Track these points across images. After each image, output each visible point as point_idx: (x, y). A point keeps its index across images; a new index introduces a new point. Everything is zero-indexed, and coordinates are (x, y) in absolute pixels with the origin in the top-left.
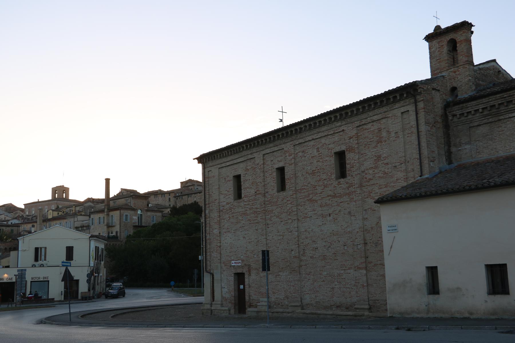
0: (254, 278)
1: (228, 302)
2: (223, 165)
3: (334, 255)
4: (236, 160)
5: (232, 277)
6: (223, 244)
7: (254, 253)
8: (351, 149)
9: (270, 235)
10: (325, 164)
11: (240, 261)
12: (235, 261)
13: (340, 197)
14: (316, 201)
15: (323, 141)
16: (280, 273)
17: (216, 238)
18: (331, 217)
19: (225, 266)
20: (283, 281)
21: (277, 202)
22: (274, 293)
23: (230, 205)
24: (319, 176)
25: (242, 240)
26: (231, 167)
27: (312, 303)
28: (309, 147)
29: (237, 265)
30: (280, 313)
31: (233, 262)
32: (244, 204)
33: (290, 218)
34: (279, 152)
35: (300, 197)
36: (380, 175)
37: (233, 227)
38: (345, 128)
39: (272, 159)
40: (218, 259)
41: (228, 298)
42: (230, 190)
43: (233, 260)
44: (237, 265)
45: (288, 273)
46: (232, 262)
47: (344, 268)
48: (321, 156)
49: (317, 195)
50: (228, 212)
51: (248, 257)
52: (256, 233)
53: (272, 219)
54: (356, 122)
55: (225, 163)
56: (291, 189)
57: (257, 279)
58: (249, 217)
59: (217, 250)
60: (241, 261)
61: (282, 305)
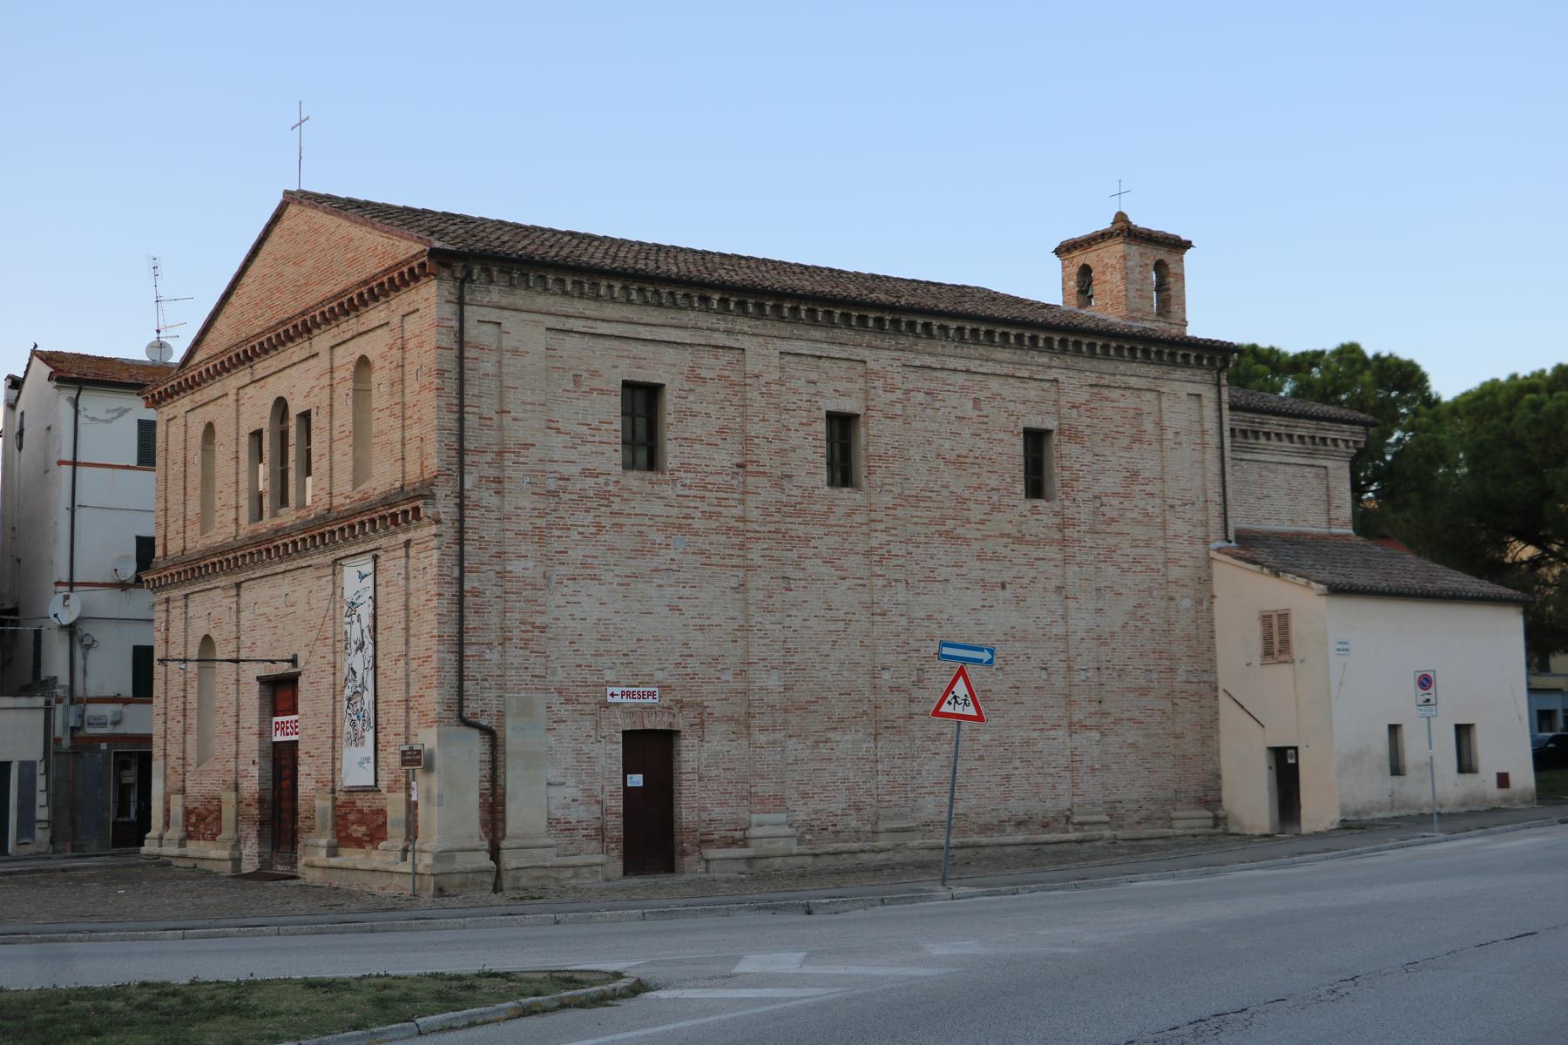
0: (719, 749)
2: (578, 325)
3: (1013, 691)
4: (648, 328)
5: (618, 743)
7: (720, 667)
8: (1074, 436)
9: (794, 612)
11: (651, 690)
12: (626, 689)
13: (1037, 543)
14: (967, 541)
15: (995, 385)
16: (830, 735)
17: (524, 593)
22: (805, 795)
23: (601, 480)
24: (979, 475)
25: (666, 617)
26: (616, 344)
28: (951, 388)
29: (637, 700)
30: (844, 856)
31: (618, 691)
32: (680, 493)
34: (845, 364)
35: (915, 520)
36: (1135, 515)
38: (1061, 378)
39: (813, 376)
43: (616, 684)
44: (637, 700)
45: (861, 734)
46: (610, 690)
47: (1041, 726)
48: (986, 423)
49: (968, 526)
54: (1087, 374)
55: (589, 323)
56: (888, 488)
57: (734, 752)
60: (656, 689)
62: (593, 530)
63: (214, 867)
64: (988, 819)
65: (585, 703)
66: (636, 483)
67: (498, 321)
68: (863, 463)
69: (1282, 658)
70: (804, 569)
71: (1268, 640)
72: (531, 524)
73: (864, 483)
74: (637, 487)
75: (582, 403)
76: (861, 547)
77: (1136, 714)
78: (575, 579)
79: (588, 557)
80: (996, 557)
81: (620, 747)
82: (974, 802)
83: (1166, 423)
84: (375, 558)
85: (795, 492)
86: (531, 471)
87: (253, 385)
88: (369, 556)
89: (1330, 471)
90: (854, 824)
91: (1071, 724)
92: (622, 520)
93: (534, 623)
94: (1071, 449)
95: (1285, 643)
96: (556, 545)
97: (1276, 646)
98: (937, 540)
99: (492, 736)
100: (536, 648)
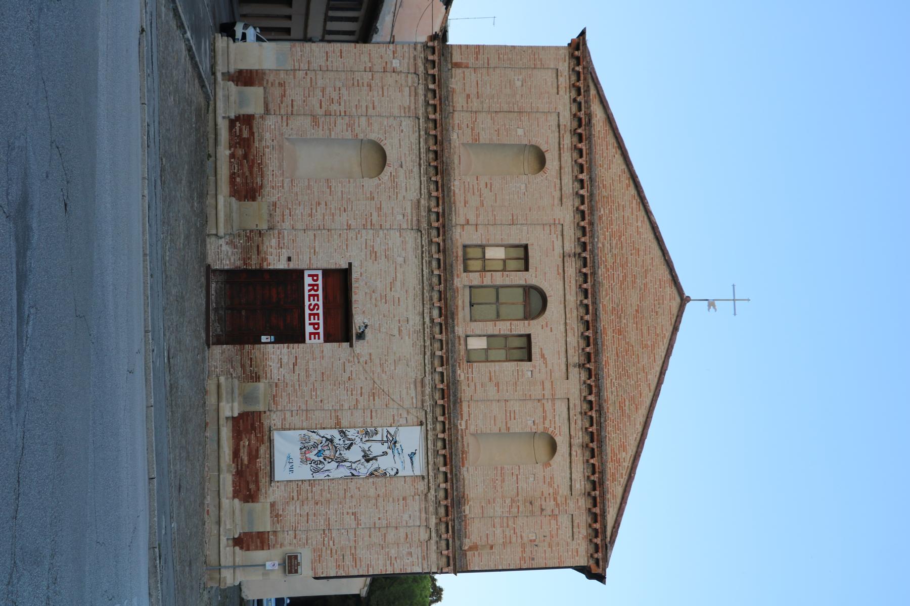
63: (212, 220)
84: (423, 477)
87: (562, 252)
88: (425, 474)
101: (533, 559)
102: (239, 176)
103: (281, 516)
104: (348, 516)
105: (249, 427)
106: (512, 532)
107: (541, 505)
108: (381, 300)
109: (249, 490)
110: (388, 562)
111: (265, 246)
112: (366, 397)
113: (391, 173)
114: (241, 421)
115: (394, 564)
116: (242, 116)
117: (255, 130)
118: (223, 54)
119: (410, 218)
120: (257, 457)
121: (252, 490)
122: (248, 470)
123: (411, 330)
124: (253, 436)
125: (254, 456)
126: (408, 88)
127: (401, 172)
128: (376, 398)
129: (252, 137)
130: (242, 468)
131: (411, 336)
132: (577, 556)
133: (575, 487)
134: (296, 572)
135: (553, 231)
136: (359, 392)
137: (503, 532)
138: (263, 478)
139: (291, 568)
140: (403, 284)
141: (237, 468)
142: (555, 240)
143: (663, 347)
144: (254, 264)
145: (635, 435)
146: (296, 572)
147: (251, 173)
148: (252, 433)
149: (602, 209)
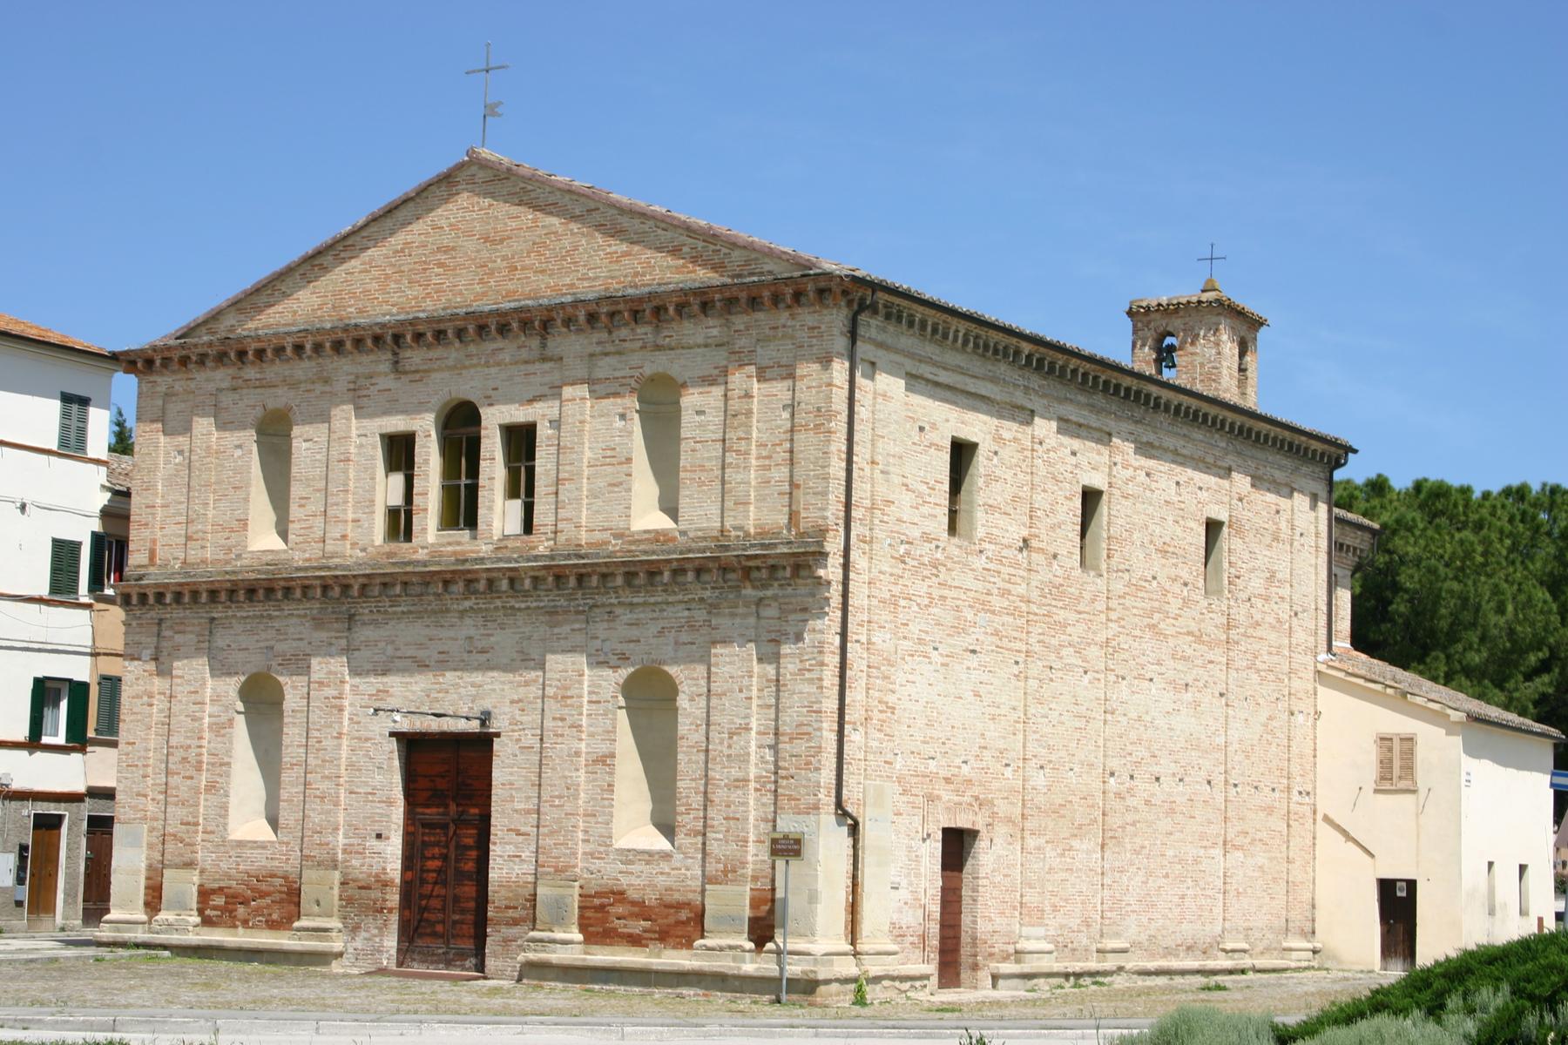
1: (908, 945)
5: (938, 841)
6: (899, 699)
8: (1239, 532)
9: (1053, 706)
10: (1189, 539)
14: (1166, 636)
17: (883, 668)
18: (1189, 695)
19: (904, 793)
20: (1081, 870)
21: (1079, 599)
22: (1055, 908)
24: (1175, 565)
27: (1140, 939)
32: (987, 566)
33: (1112, 667)
37: (940, 642)
40: (886, 762)
41: (908, 928)
42: (938, 486)
47: (1205, 843)
48: (1183, 510)
50: (925, 573)
51: (986, 773)
52: (1016, 688)
53: (1064, 652)
58: (998, 624)
59: (884, 721)
61: (1074, 950)
62: (926, 601)
64: (1170, 943)
65: (916, 795)
66: (956, 552)
67: (873, 360)
68: (1104, 545)
69: (1403, 784)
70: (1061, 658)
71: (1385, 766)
72: (889, 591)
73: (1104, 566)
74: (958, 557)
75: (925, 458)
76: (1101, 637)
77: (1263, 835)
78: (912, 655)
79: (923, 631)
80: (1184, 658)
81: (939, 845)
82: (1161, 922)
83: (1296, 523)
85: (1060, 572)
86: (892, 531)
89: (1339, 579)
90: (1085, 941)
91: (1225, 843)
92: (946, 592)
93: (887, 703)
94: (1237, 544)
95: (1409, 768)
96: (901, 616)
97: (1396, 772)
98: (1148, 634)
99: (854, 830)
100: (888, 731)
101: (819, 409)
102: (270, 915)
103: (725, 866)
104: (734, 746)
105: (599, 915)
106: (778, 449)
107: (739, 398)
108: (440, 683)
109: (689, 920)
110: (807, 675)
111: (361, 876)
112: (566, 711)
113: (279, 665)
114: (591, 929)
115: (810, 665)
116: (200, 906)
117: (216, 886)
118: (118, 930)
119: (333, 634)
120: (641, 904)
121: (689, 915)
122: (660, 921)
123: (482, 631)
124: (612, 910)
125: (641, 910)
126: (177, 636)
127: (280, 647)
128: (569, 694)
129: (225, 890)
130: (655, 932)
131: (490, 632)
132: (819, 328)
133: (715, 337)
134: (798, 842)
135: (365, 392)
136: (560, 724)
137: (777, 465)
138: (672, 895)
139: (792, 850)
140: (421, 646)
141: (655, 939)
142: (378, 387)
143: (539, 190)
144: (394, 898)
145: (660, 232)
146: (798, 842)
147: (268, 894)
148: (608, 912)
149: (350, 310)
